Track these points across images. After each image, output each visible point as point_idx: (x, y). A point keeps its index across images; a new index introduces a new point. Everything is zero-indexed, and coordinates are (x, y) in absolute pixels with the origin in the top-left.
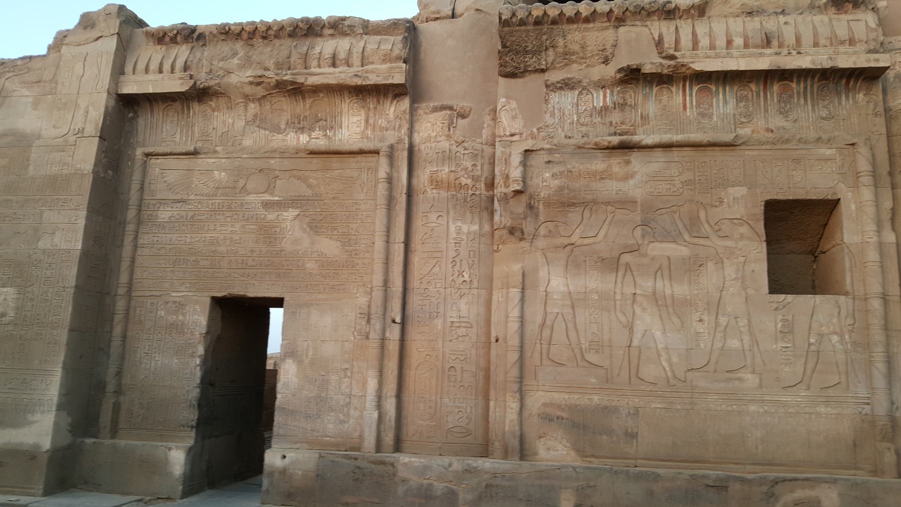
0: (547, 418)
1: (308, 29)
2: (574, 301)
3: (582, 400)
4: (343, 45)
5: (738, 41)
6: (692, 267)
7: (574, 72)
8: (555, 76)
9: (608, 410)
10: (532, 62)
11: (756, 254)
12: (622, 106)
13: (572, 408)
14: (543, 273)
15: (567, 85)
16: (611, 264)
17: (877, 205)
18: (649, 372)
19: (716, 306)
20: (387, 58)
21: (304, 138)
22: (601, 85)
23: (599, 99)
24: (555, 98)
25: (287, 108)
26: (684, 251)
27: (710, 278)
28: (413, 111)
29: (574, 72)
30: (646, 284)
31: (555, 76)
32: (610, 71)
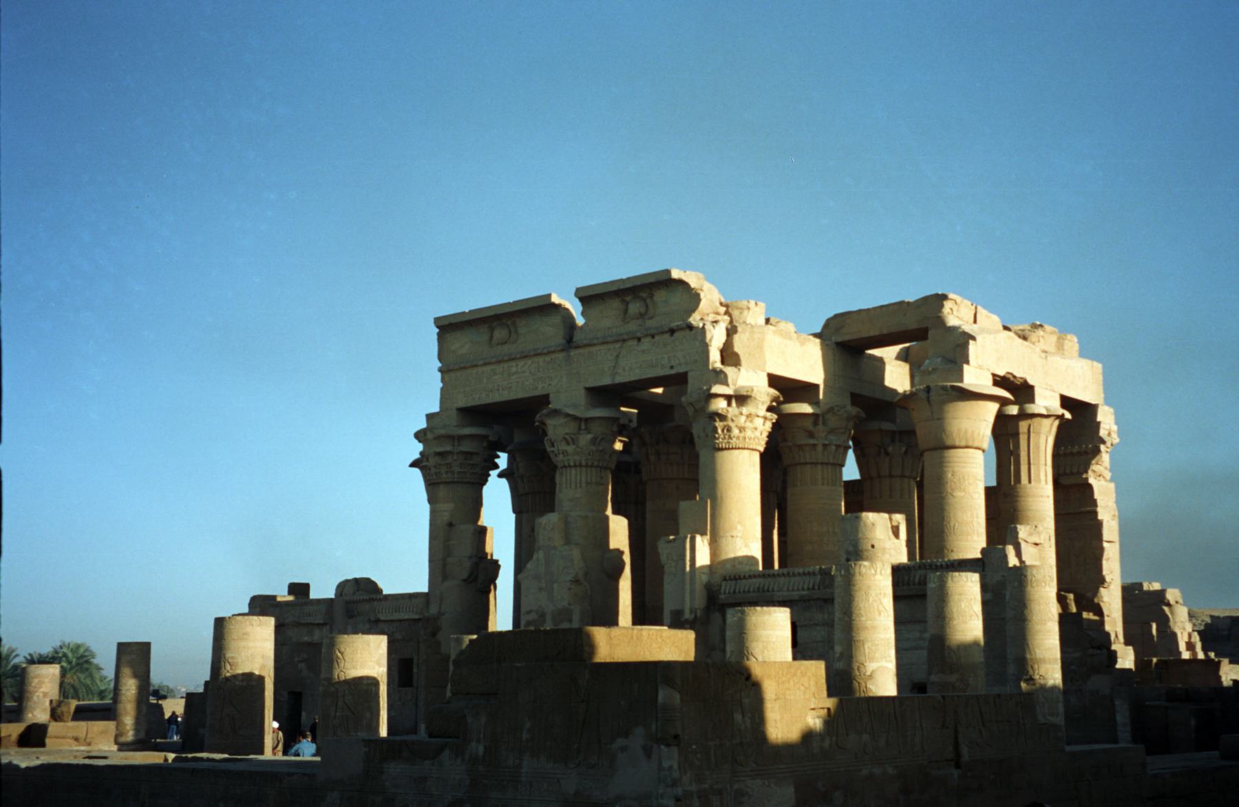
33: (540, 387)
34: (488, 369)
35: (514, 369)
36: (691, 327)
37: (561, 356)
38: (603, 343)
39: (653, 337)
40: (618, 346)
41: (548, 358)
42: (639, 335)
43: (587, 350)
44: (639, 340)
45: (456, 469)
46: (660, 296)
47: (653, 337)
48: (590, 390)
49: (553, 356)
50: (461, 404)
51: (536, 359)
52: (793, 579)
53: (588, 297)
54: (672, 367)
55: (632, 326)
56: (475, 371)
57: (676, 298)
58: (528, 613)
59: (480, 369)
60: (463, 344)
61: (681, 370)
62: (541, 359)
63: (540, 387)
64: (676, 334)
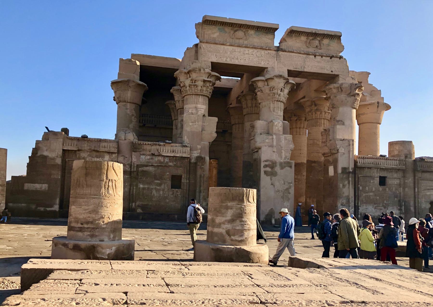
0: (138, 206)
1: (100, 141)
2: (144, 189)
3: (144, 203)
4: (106, 144)
5: (169, 151)
6: (160, 185)
7: (144, 152)
8: (141, 153)
9: (147, 205)
10: (138, 150)
11: (169, 183)
12: (152, 159)
13: (142, 205)
14: (139, 184)
15: (143, 155)
16: (150, 183)
17: (187, 176)
18: (154, 199)
19: (163, 190)
20: (114, 147)
21: (98, 159)
22: (149, 155)
23: (148, 157)
24: (141, 156)
25: (95, 154)
26: (159, 182)
27: (163, 187)
28: (118, 155)
29: (144, 152)
30: (154, 187)
31: (141, 153)
32: (150, 153)
33: (263, 63)
34: (231, 48)
35: (247, 52)
36: (341, 57)
37: (274, 52)
38: (299, 53)
39: (322, 57)
40: (305, 56)
41: (266, 52)
42: (317, 54)
43: (288, 54)
44: (315, 56)
45: (209, 89)
46: (326, 41)
47: (322, 57)
48: (289, 71)
49: (269, 51)
50: (215, 60)
51: (259, 50)
52: (388, 161)
53: (293, 33)
54: (332, 71)
55: (311, 50)
56: (222, 47)
57: (334, 44)
58: (266, 161)
59: (226, 47)
60: (214, 33)
61: (336, 73)
62: (263, 52)
63: (263, 63)
64: (333, 59)
